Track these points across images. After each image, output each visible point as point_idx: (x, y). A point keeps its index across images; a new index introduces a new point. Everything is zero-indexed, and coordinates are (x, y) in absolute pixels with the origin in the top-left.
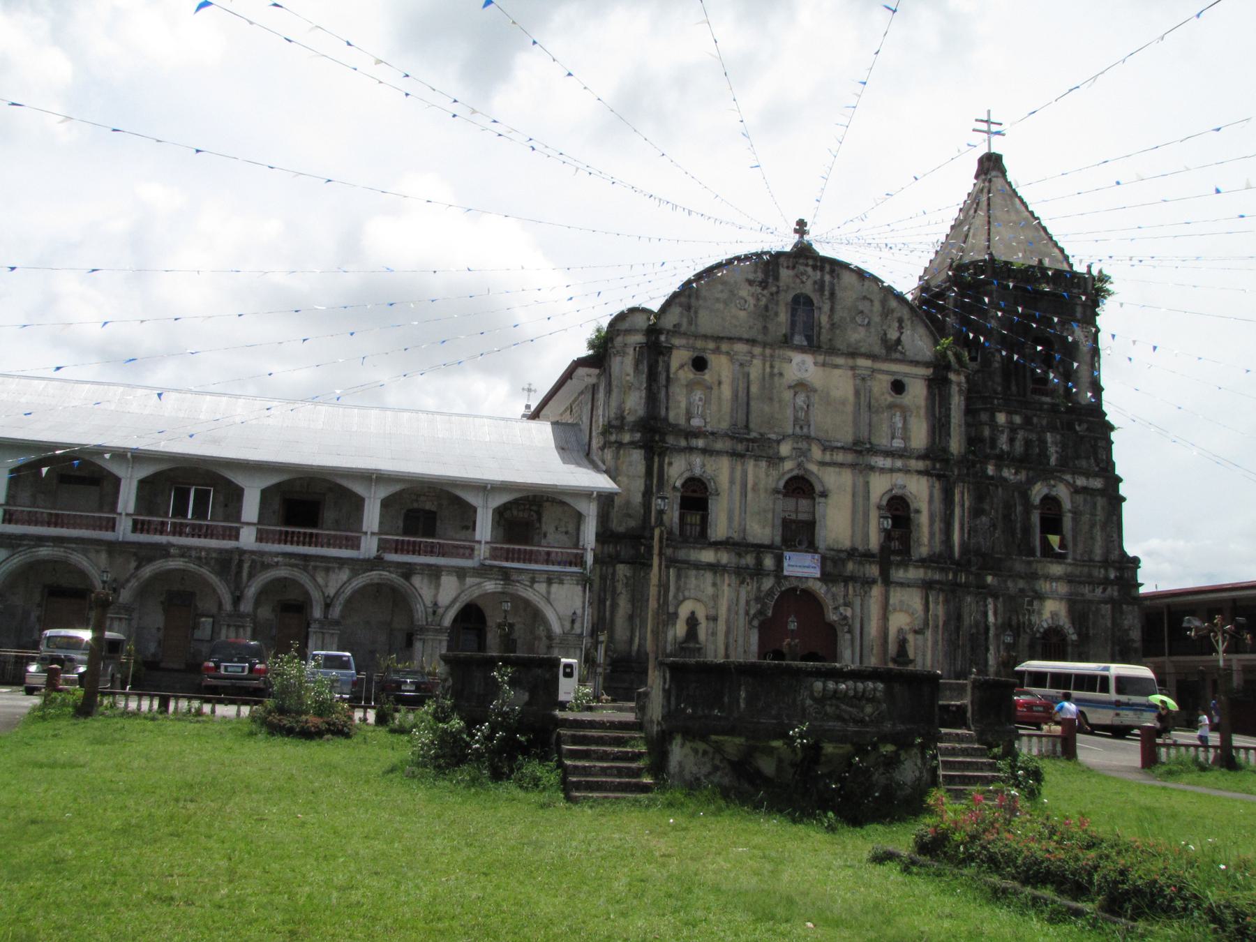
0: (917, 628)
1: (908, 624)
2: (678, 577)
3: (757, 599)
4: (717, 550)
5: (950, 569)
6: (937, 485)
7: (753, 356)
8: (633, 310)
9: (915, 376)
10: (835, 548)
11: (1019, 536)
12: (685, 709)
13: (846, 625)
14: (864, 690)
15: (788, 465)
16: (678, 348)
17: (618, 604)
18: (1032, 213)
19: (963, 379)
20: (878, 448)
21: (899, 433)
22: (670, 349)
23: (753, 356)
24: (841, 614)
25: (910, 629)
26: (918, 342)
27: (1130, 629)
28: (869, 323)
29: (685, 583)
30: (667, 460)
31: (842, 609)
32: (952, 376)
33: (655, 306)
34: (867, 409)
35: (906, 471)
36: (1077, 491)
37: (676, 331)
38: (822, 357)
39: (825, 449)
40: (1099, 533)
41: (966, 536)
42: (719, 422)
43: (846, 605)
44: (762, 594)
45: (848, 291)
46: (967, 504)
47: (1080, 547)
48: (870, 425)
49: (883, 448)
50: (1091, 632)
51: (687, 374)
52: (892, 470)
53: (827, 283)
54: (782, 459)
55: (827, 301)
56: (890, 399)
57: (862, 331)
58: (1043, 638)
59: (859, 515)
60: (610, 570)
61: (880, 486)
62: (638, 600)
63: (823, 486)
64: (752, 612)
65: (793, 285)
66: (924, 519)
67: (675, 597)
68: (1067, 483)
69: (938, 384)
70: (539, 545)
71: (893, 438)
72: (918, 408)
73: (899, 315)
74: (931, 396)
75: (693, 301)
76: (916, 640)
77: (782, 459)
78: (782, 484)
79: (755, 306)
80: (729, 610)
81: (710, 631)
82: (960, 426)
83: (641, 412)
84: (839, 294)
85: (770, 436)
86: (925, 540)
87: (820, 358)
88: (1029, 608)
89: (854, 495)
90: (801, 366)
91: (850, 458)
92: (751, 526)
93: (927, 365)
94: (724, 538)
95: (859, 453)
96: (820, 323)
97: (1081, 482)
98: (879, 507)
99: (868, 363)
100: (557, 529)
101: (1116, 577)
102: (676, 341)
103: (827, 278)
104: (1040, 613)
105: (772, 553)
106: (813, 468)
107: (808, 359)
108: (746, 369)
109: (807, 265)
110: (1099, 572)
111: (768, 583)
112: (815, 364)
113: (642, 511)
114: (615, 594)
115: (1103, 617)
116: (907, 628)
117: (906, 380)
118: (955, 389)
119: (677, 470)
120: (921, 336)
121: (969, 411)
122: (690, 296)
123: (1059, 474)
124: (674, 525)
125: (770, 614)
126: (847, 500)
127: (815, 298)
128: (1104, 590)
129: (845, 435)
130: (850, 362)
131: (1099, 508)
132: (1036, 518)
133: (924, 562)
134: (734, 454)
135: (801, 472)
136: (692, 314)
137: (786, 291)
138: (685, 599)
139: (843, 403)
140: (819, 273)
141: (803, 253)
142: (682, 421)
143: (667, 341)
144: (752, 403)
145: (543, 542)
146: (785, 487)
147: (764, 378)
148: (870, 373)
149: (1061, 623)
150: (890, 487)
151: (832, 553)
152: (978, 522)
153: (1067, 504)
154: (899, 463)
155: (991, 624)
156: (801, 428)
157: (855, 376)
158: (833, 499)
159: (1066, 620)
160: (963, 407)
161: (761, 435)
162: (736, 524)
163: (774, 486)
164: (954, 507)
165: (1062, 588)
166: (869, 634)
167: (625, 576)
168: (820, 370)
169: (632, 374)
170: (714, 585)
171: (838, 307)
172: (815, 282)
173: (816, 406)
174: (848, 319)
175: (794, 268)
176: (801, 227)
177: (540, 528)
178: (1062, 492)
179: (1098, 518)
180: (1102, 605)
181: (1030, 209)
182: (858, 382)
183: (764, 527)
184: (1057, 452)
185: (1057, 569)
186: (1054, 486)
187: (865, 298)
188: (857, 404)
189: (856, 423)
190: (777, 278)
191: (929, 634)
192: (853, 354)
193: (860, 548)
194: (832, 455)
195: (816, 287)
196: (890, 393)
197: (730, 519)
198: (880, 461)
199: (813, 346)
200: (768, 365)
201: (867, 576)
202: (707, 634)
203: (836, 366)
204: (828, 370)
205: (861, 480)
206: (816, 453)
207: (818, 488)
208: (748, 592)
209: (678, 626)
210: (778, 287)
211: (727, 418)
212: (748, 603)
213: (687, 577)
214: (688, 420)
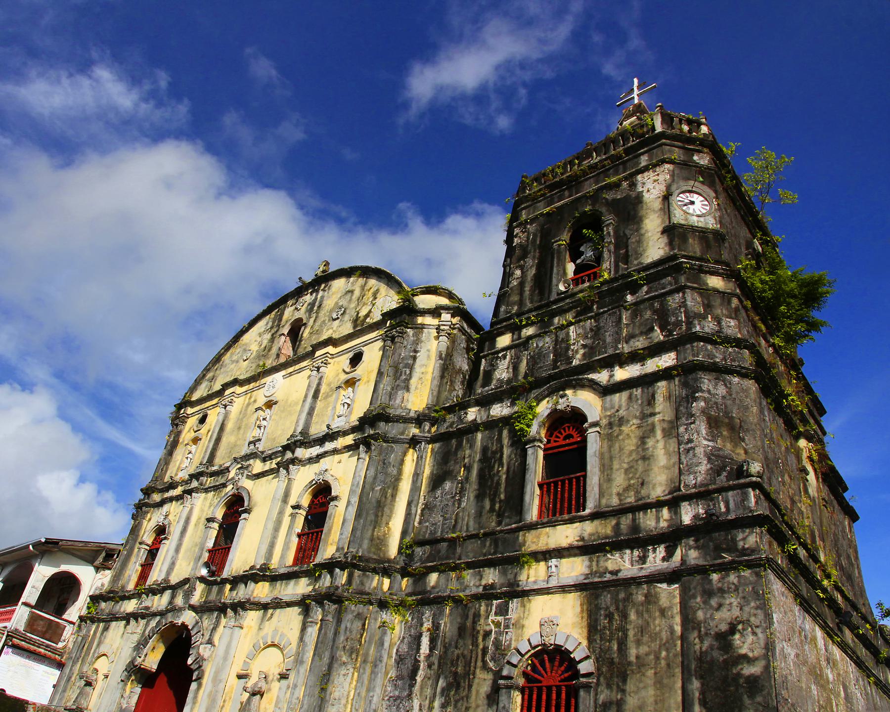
11: (502, 496)
27: (732, 630)
40: (661, 445)
46: (427, 471)
47: (619, 480)
50: (633, 652)
54: (224, 485)
88: (500, 618)
92: (181, 565)
101: (696, 517)
104: (519, 625)
106: (247, 484)
110: (658, 520)
115: (663, 612)
128: (669, 554)
131: (660, 398)
147: (241, 412)
161: (221, 466)
179: (657, 418)
180: (664, 586)
184: (584, 346)
203: (301, 370)
207: (246, 504)
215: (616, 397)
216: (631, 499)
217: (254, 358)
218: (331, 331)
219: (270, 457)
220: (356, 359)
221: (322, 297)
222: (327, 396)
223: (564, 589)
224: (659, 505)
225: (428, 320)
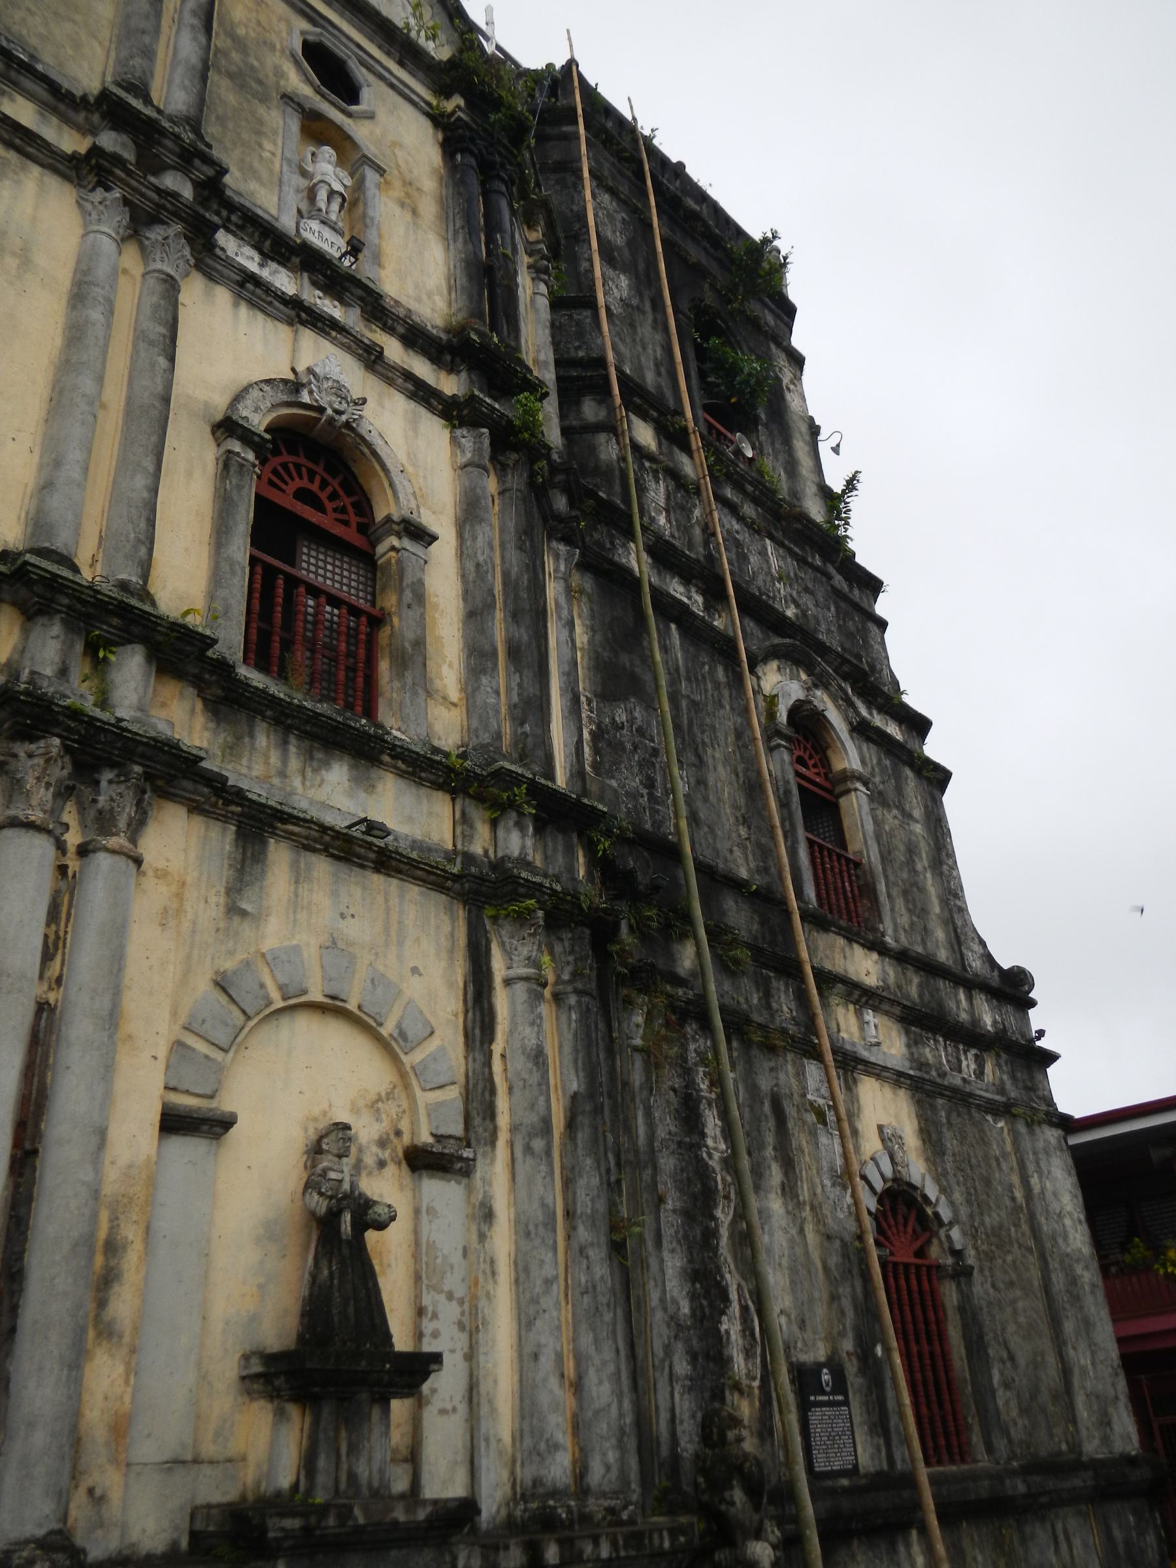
0: (425, 1138)
1: (375, 1106)
25: (382, 1143)
56: (298, 82)
149: (916, 1179)
155: (715, 1163)
196: (297, 63)
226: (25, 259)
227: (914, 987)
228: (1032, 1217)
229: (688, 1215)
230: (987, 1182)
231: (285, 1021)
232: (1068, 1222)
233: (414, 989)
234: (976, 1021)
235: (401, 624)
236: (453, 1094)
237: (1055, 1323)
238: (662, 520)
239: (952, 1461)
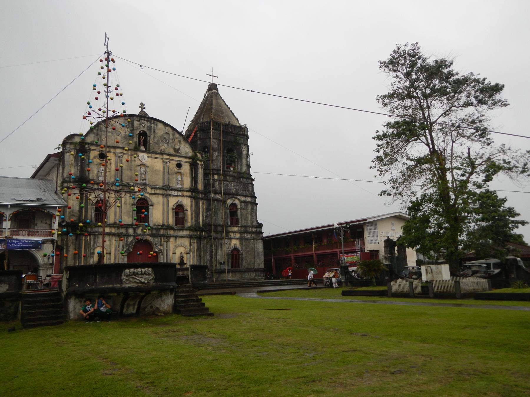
2: (95, 239)
3: (127, 245)
4: (111, 227)
5: (198, 230)
6: (194, 201)
7: (124, 154)
8: (73, 136)
9: (186, 162)
10: (157, 224)
12: (75, 285)
13: (161, 252)
14: (145, 271)
15: (139, 195)
16: (93, 150)
17: (69, 250)
18: (227, 105)
19: (202, 163)
20: (172, 188)
21: (180, 182)
22: (91, 150)
23: (124, 154)
24: (159, 249)
26: (186, 149)
28: (168, 142)
29: (98, 240)
30: (89, 194)
31: (159, 247)
32: (199, 162)
33: (84, 134)
34: (167, 174)
35: (183, 196)
36: (241, 202)
37: (92, 144)
38: (151, 154)
39: (152, 189)
41: (204, 218)
42: (110, 179)
43: (161, 245)
44: (128, 243)
45: (160, 130)
46: (204, 207)
47: (243, 221)
48: (169, 179)
49: (174, 188)
51: (97, 161)
52: (177, 196)
53: (152, 127)
55: (153, 134)
56: (176, 170)
57: (166, 145)
58: (231, 253)
59: (165, 213)
60: (65, 237)
61: (173, 201)
62: (79, 248)
63: (151, 202)
64: (125, 250)
65: (139, 127)
66: (189, 213)
67: (93, 246)
68: (239, 200)
69: (193, 165)
70: (34, 229)
71: (177, 184)
72: (187, 173)
73: (179, 140)
74: (191, 169)
75: (99, 132)
76: (187, 256)
77: (136, 192)
78: (136, 201)
79: (124, 135)
80: (115, 249)
81: (108, 258)
82: (201, 180)
83: (78, 174)
84: (157, 131)
85: (130, 184)
86: (190, 220)
87: (150, 155)
89: (163, 205)
90: (144, 157)
91: (161, 192)
93: (189, 158)
94: (113, 223)
95: (166, 190)
96: (150, 142)
97: (243, 199)
98: (173, 209)
99: (168, 157)
100: (42, 222)
102: (92, 148)
103: (152, 125)
105: (132, 227)
106: (148, 195)
107: (145, 155)
108: (121, 159)
109: (145, 120)
111: (130, 239)
112: (148, 157)
113: (79, 214)
114: (68, 246)
116: (184, 252)
117: (182, 163)
118: (200, 166)
119: (93, 197)
120: (187, 148)
121: (206, 175)
122: (97, 130)
123: (236, 196)
124: (92, 218)
125: (131, 250)
126: (161, 207)
127: (148, 133)
129: (160, 184)
130: (161, 157)
132: (228, 211)
133: (189, 229)
134: (116, 191)
135: (143, 197)
136: (99, 137)
137: (136, 130)
138: (97, 247)
139: (159, 171)
140: (149, 123)
141: (143, 116)
142: (95, 178)
143: (88, 147)
144: (124, 171)
145: (36, 227)
146: (137, 202)
148: (169, 160)
149: (237, 247)
150: (177, 202)
151: (156, 226)
152: (208, 213)
153: (239, 207)
154: (180, 193)
156: (143, 180)
157: (163, 162)
158: (155, 207)
159: (239, 246)
160: (203, 173)
161: (127, 183)
162: (117, 217)
163: (132, 202)
164: (200, 208)
165: (238, 236)
166: (170, 255)
167: (72, 239)
168: (150, 159)
169: (74, 160)
170: (110, 240)
171: (156, 136)
172: (148, 127)
173: (148, 172)
174: (160, 141)
175: (139, 121)
176: (142, 106)
177: (34, 222)
178: (237, 202)
179: (249, 211)
181: (226, 104)
182: (164, 164)
183: (129, 218)
185: (236, 229)
186: (234, 200)
187: (167, 133)
188: (164, 172)
189: (164, 179)
190: (133, 124)
191: (191, 254)
192: (162, 153)
193: (166, 224)
194: (155, 190)
195: (148, 128)
197: (115, 215)
198: (173, 193)
199: (147, 151)
200: (130, 157)
201: (168, 234)
202: (107, 259)
203: (156, 158)
204: (153, 159)
205: (165, 199)
206: (149, 190)
207: (150, 203)
208: (123, 242)
209: (95, 257)
210: (133, 128)
211: (113, 176)
212: (123, 247)
213: (98, 238)
214: (98, 178)
215: (242, 204)
216: (245, 225)
217: (124, 137)
218: (163, 147)
219: (155, 188)
220: (179, 166)
221: (154, 127)
222: (172, 175)
223: (237, 239)
224: (249, 227)
225: (199, 162)
226: (160, 204)
227: (243, 229)
228: (254, 249)
229: (210, 253)
230: (248, 246)
231: (179, 248)
232: (260, 249)
233: (186, 244)
234: (252, 231)
235: (186, 218)
236: (189, 250)
237: (254, 258)
238: (217, 187)
239: (236, 268)
